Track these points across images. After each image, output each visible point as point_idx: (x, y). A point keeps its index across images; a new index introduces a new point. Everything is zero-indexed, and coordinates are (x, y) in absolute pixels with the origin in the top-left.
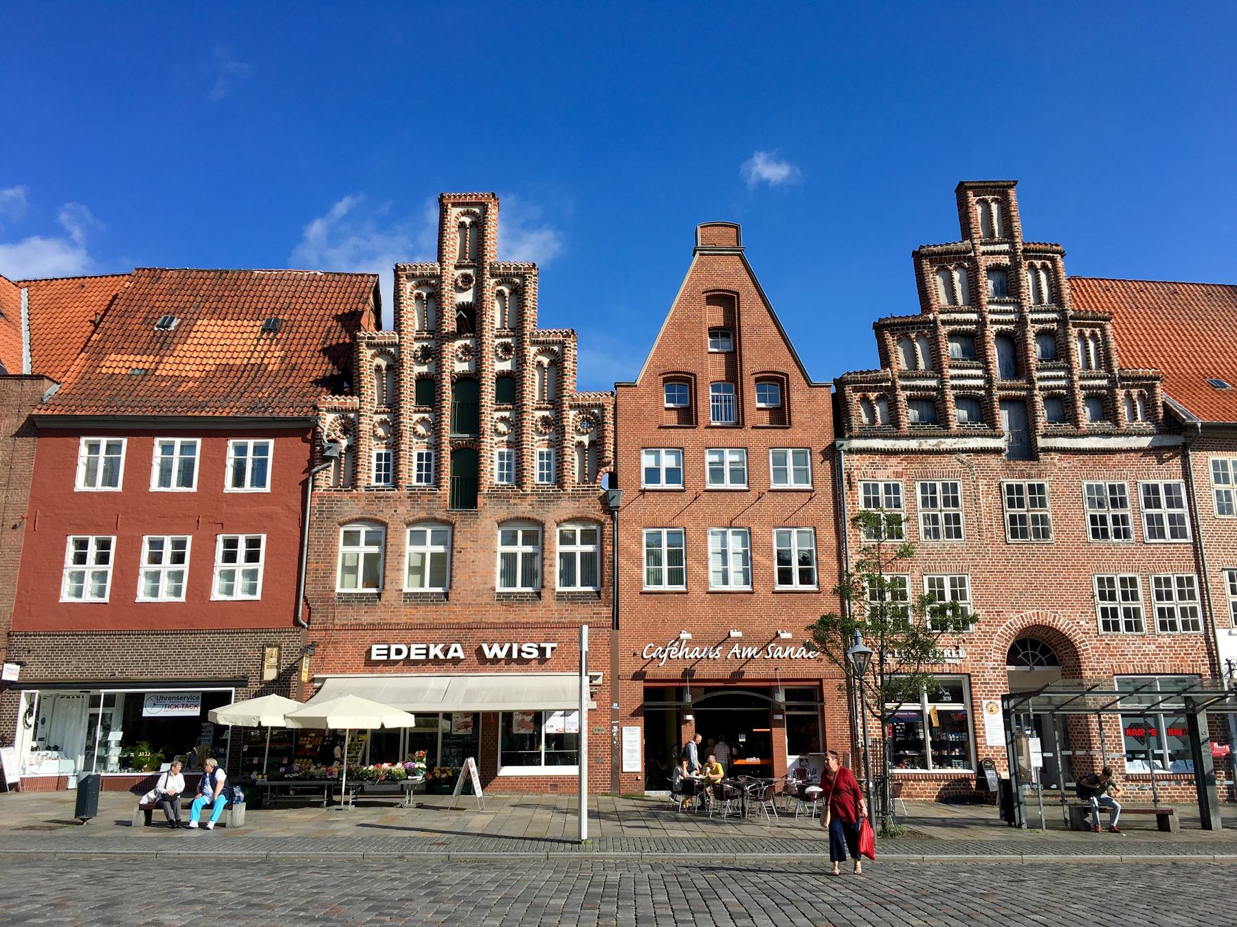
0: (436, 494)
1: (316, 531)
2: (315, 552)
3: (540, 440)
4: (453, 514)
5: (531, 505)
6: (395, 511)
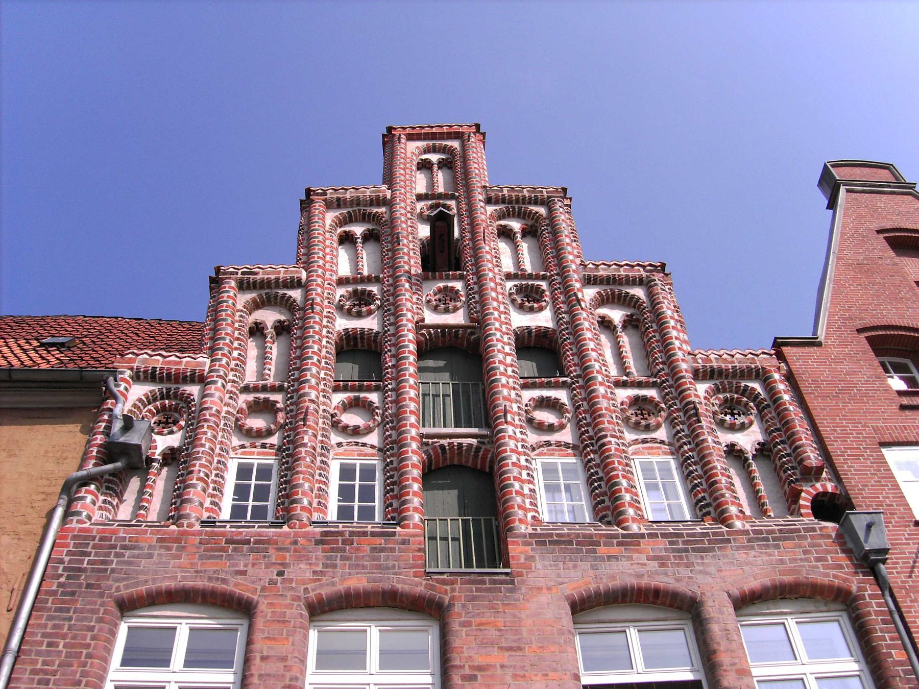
0: (394, 534)
1: (50, 618)
2: (34, 672)
3: (636, 442)
4: (444, 582)
5: (655, 558)
6: (281, 573)
